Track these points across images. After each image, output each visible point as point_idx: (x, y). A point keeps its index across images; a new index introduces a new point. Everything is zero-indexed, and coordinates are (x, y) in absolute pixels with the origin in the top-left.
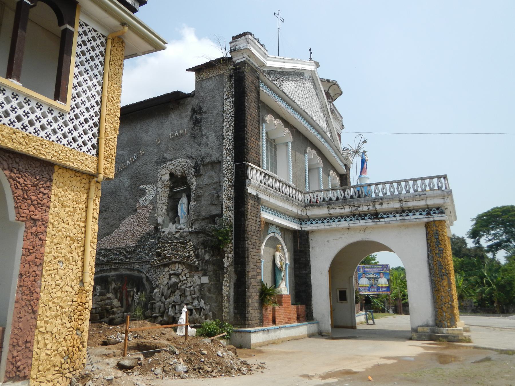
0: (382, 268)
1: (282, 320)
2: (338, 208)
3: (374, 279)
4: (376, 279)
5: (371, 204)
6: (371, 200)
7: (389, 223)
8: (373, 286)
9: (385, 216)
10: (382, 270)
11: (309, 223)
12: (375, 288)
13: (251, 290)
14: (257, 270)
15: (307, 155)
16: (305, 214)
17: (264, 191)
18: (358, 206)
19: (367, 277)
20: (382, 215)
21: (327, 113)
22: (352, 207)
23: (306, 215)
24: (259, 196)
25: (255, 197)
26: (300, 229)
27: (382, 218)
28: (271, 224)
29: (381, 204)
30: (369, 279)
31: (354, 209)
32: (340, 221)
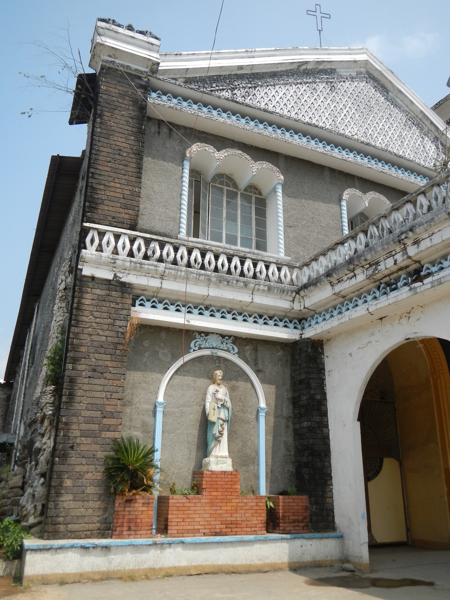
1: (199, 527)
2: (345, 278)
5: (398, 249)
6: (393, 240)
7: (441, 283)
9: (434, 269)
11: (313, 322)
13: (73, 459)
14: (105, 420)
15: (344, 203)
16: (302, 308)
17: (135, 269)
18: (377, 263)
20: (428, 269)
21: (433, 129)
22: (367, 269)
23: (305, 308)
24: (123, 280)
25: (113, 283)
26: (297, 337)
27: (429, 275)
28: (200, 333)
29: (416, 242)
31: (370, 272)
32: (357, 305)
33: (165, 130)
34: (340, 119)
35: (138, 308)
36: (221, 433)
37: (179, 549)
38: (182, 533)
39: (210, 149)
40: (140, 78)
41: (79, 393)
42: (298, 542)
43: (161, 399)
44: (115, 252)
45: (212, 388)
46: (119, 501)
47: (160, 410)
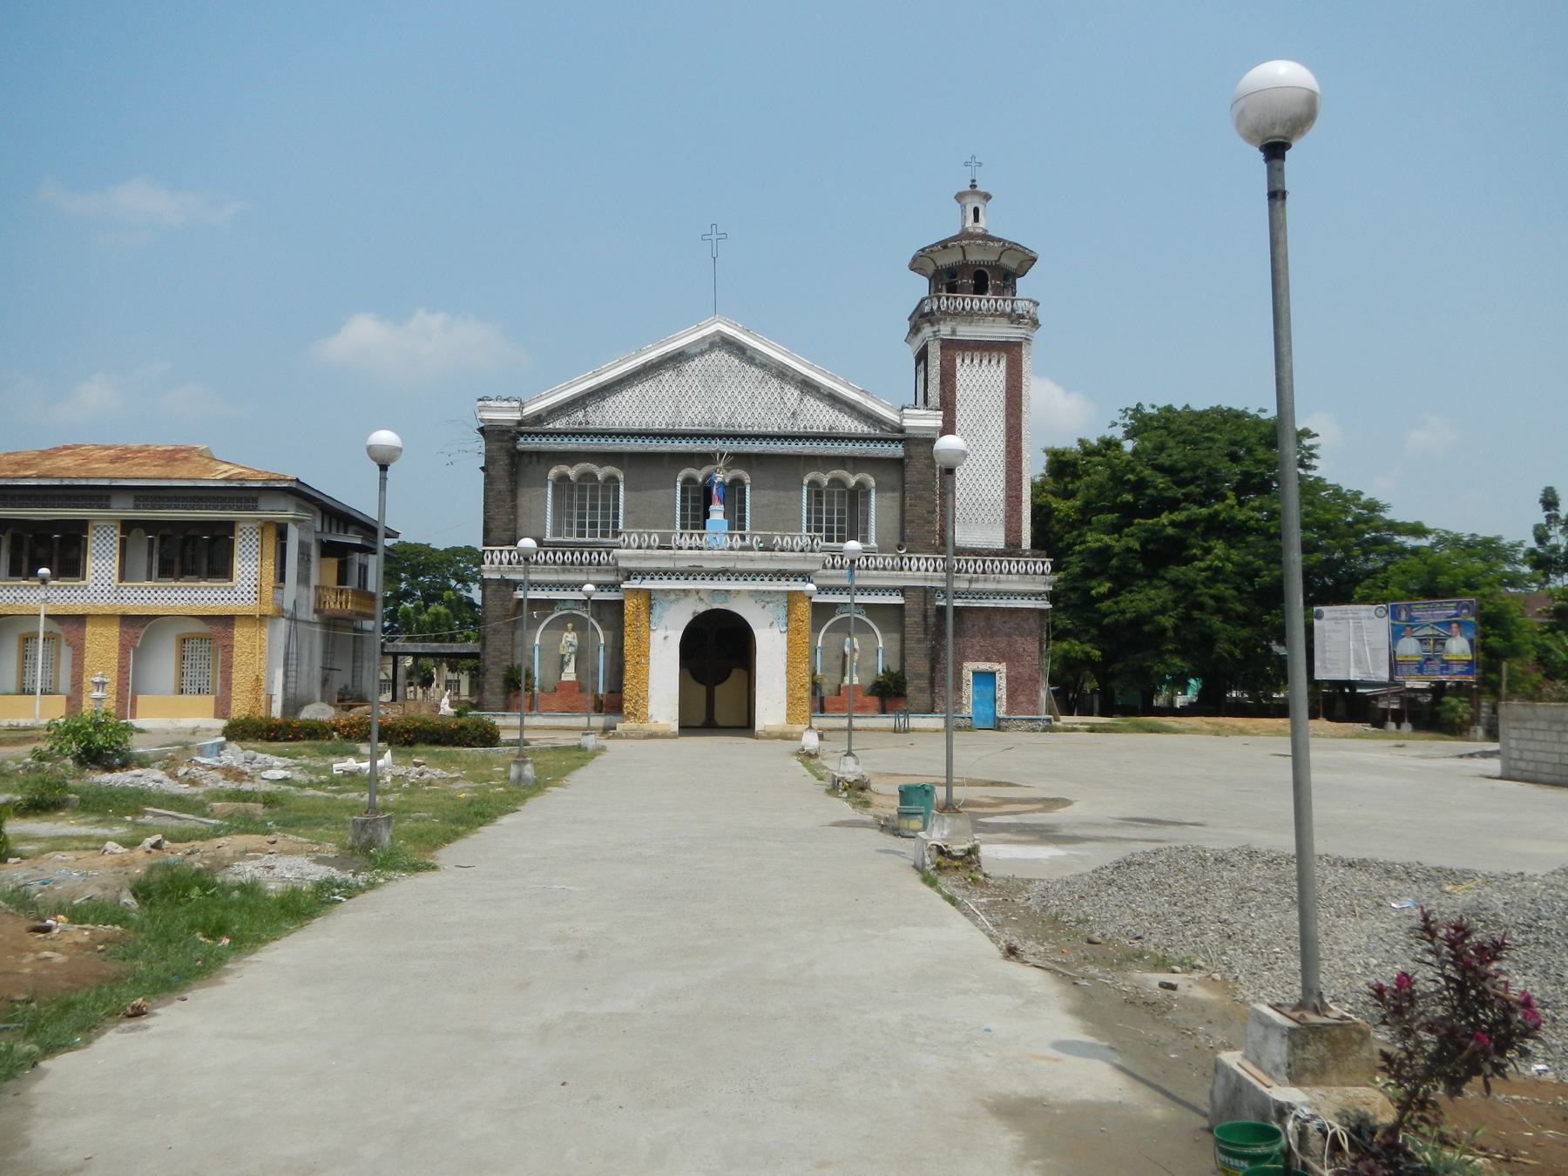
0: (1456, 608)
3: (1435, 640)
4: (1440, 641)
8: (1429, 659)
10: (1456, 616)
12: (1436, 665)
13: (488, 676)
19: (1417, 634)
30: (1422, 640)
33: (535, 459)
34: (683, 403)
35: (518, 592)
36: (569, 661)
37: (540, 718)
38: (545, 711)
39: (564, 468)
40: (510, 431)
41: (488, 643)
42: (608, 717)
43: (537, 642)
44: (501, 562)
45: (566, 634)
46: (511, 696)
47: (537, 648)
